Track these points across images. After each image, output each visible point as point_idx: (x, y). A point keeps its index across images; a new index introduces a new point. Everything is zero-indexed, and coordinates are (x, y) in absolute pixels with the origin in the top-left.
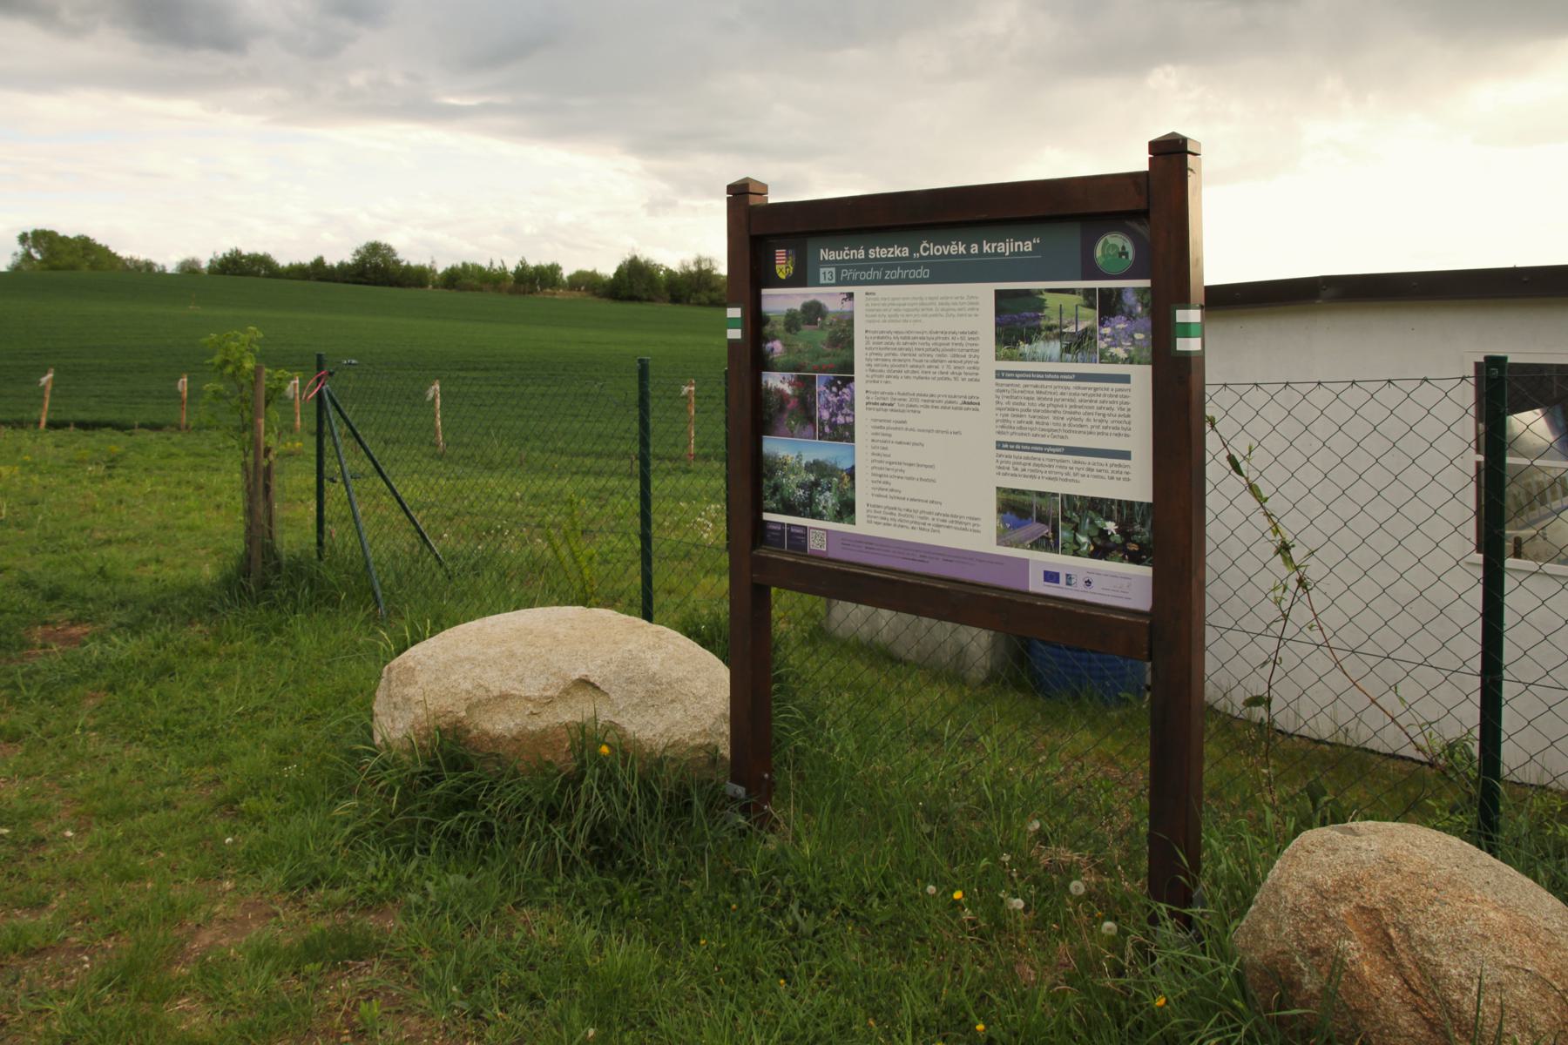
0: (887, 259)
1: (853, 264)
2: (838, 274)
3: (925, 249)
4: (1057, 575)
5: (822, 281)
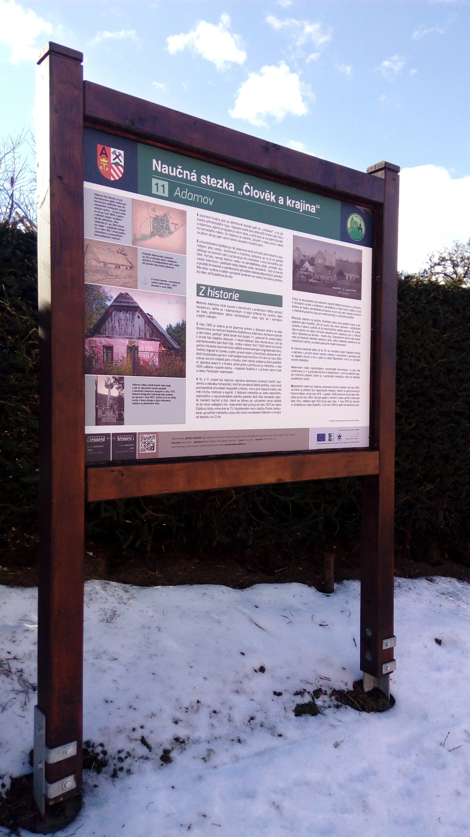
0: (216, 188)
1: (184, 184)
2: (172, 189)
3: (247, 191)
4: (324, 435)
5: (154, 191)
